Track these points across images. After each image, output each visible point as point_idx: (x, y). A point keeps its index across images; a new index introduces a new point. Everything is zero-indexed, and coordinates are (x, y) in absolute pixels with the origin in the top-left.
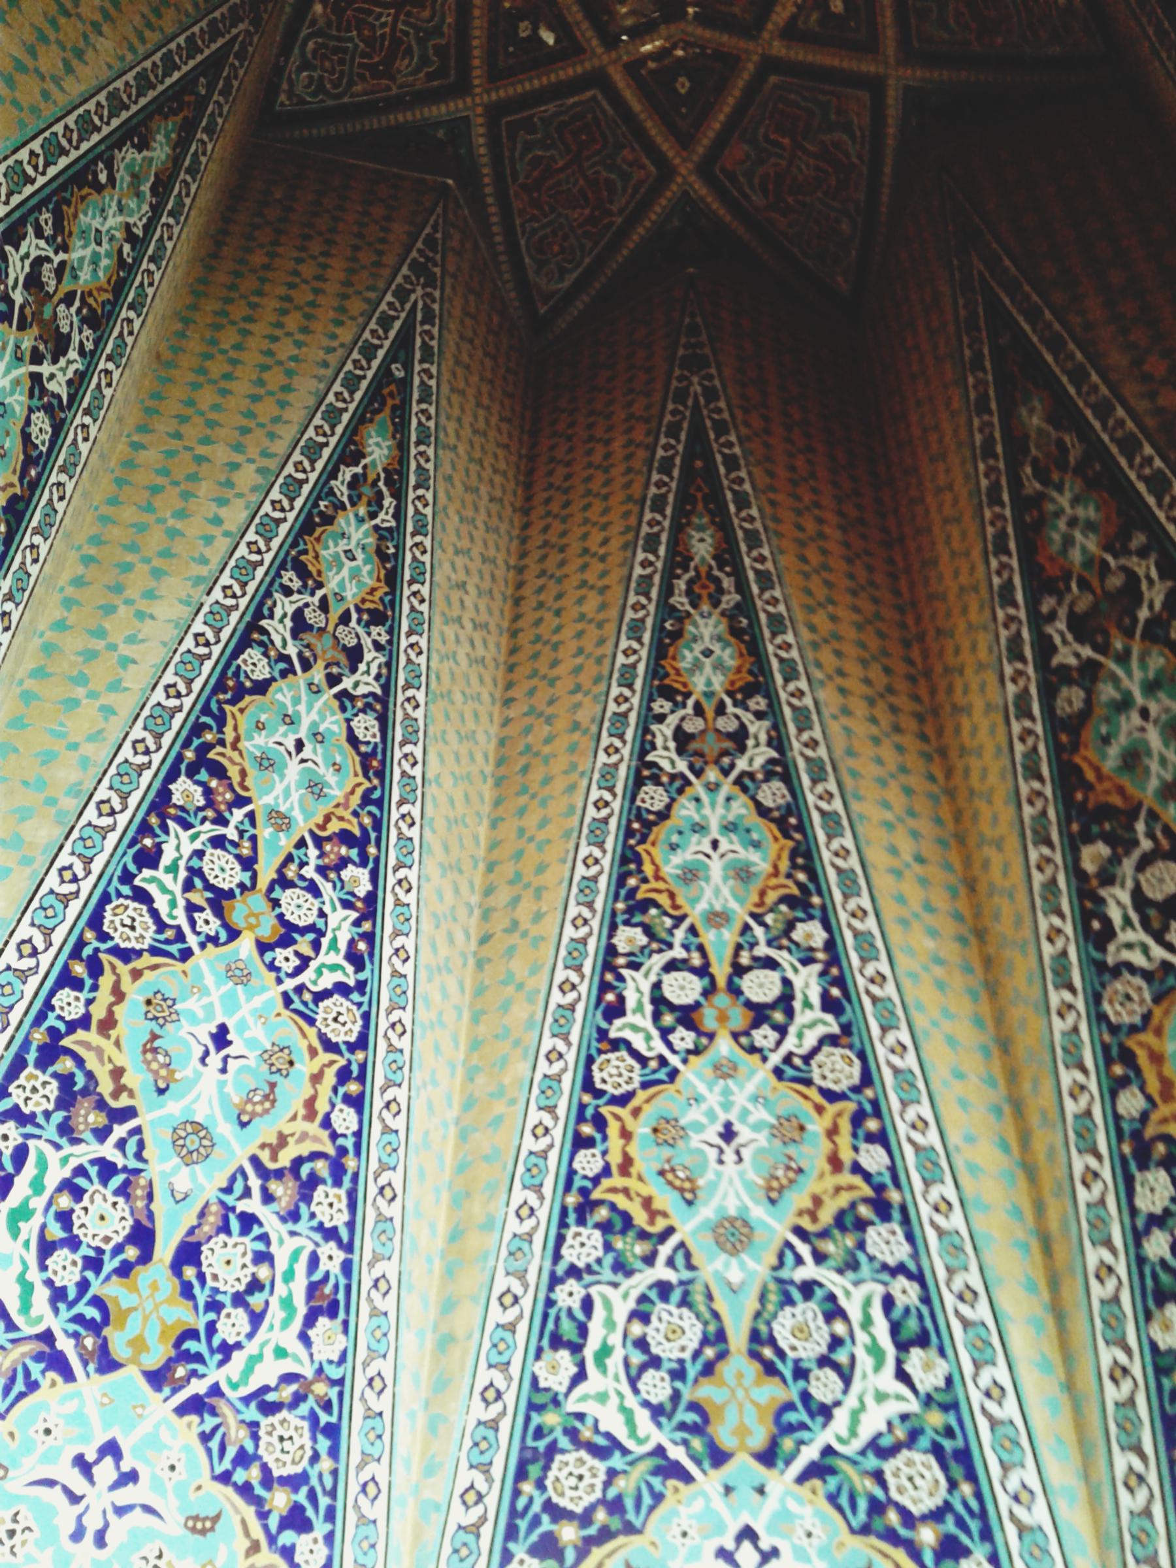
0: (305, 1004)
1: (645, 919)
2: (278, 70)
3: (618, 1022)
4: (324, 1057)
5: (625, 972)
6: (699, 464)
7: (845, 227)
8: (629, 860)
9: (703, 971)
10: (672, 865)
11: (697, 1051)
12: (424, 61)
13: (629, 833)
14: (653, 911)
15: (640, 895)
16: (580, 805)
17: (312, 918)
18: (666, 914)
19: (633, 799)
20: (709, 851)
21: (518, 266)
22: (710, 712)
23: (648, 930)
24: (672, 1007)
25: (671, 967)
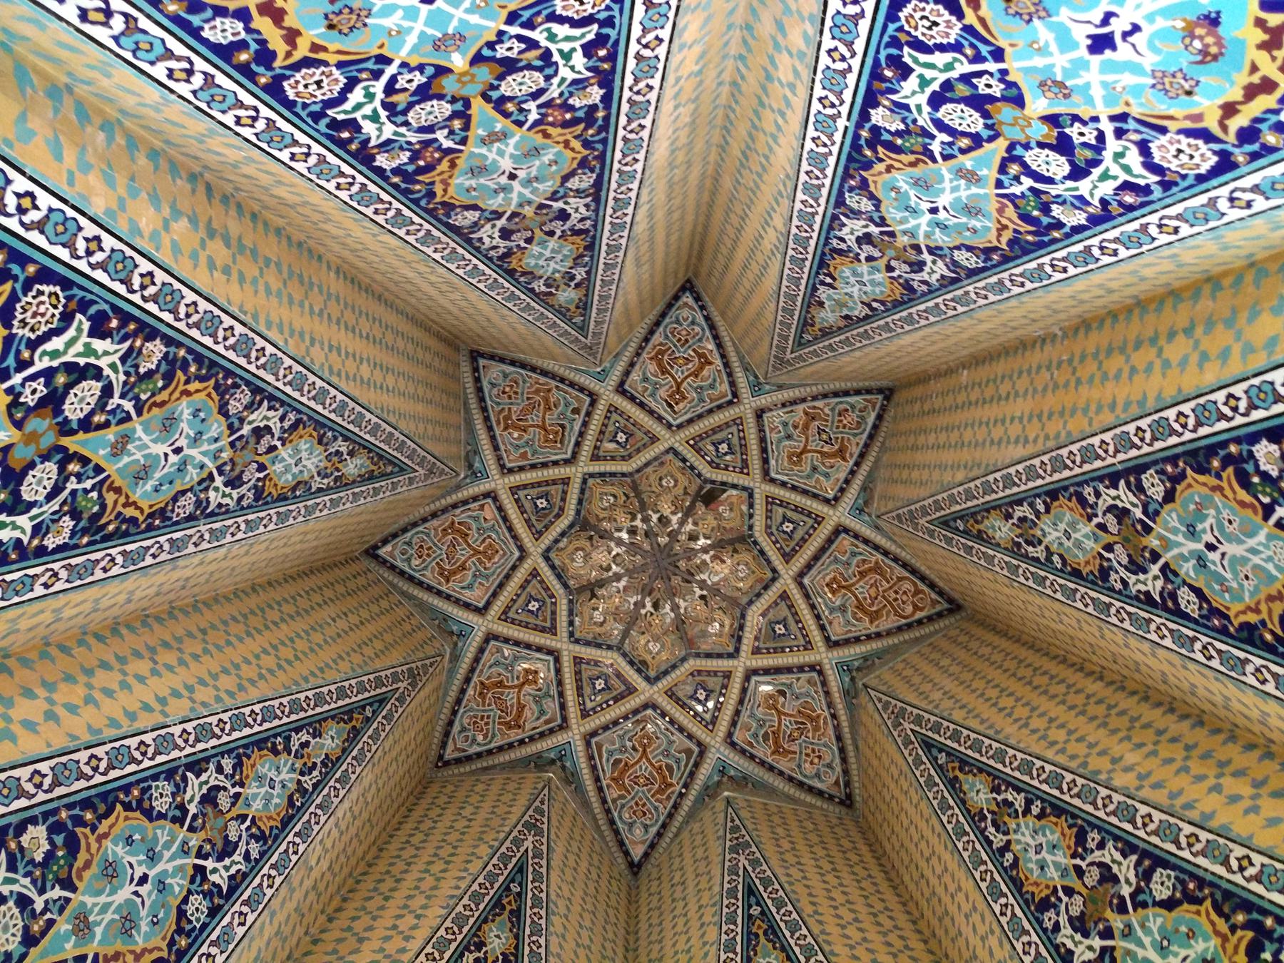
0: (360, 71)
1: (158, 376)
2: (702, 308)
3: (86, 325)
4: (302, 51)
5: (127, 345)
6: (389, 469)
7: (415, 562)
8: (209, 367)
9: (86, 424)
10: (184, 409)
11: (14, 404)
12: (646, 379)
13: (229, 373)
14: (160, 384)
15: (179, 373)
16: (269, 334)
17: (411, 116)
18: (153, 395)
19: (248, 383)
20: (177, 444)
21: (513, 363)
22: (261, 459)
23: (150, 374)
24: (69, 386)
25: (107, 391)
